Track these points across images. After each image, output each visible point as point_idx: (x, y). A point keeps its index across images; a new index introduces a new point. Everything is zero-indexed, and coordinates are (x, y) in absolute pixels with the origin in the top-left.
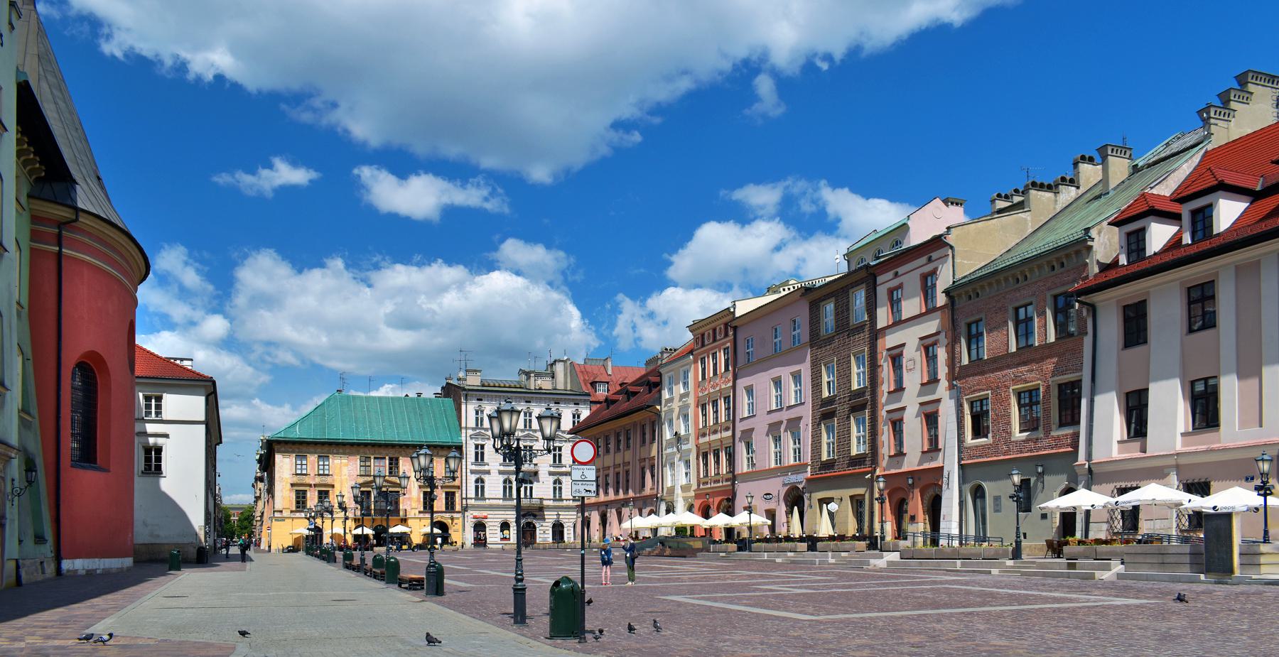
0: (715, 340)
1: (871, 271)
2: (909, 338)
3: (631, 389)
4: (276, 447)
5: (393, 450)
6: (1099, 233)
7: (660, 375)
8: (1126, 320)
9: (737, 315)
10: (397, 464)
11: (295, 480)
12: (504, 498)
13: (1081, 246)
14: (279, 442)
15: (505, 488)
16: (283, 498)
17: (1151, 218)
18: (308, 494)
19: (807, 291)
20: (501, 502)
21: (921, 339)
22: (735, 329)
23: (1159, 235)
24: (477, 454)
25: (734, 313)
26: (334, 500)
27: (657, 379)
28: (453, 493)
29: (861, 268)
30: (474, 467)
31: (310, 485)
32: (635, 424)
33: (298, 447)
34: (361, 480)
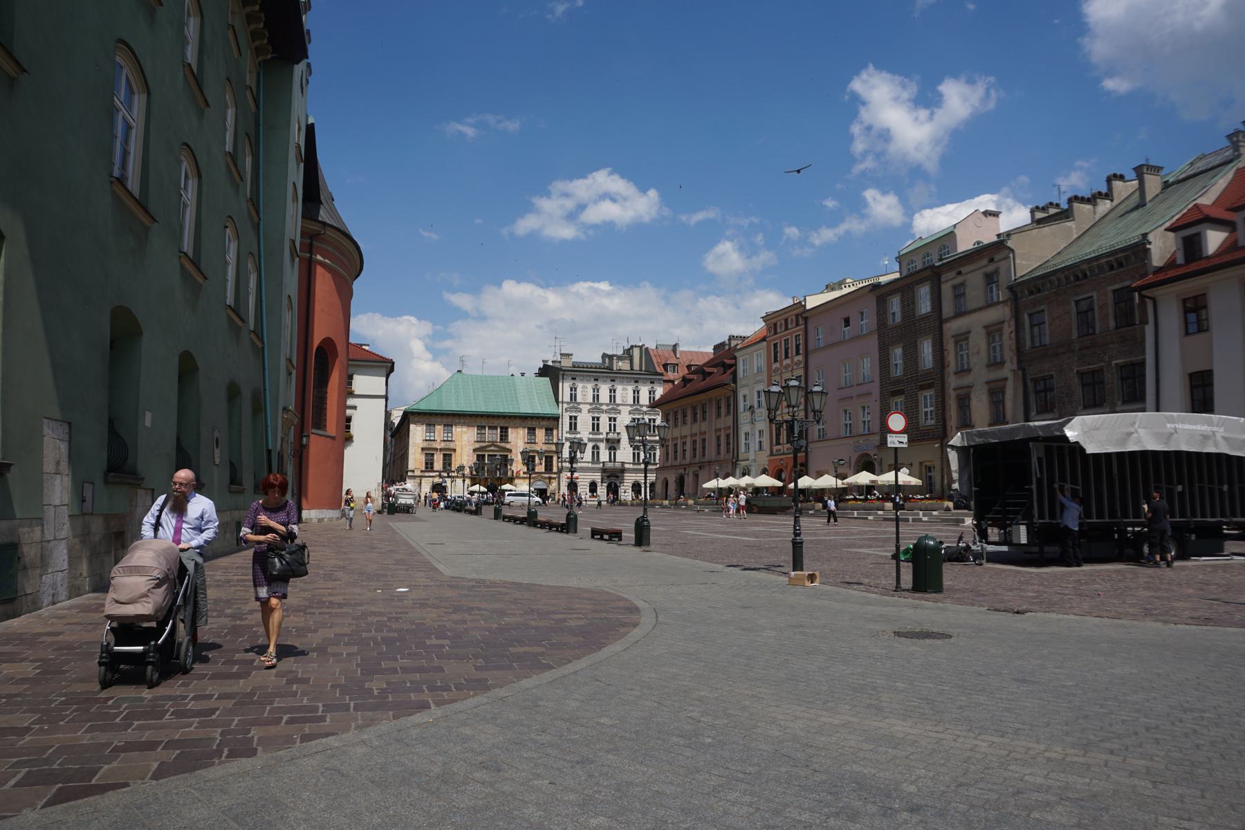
0: (786, 329)
2: (975, 323)
3: (708, 370)
4: (411, 418)
5: (502, 421)
7: (735, 358)
8: (1186, 311)
11: (425, 445)
12: (593, 462)
13: (1140, 249)
17: (1204, 225)
19: (876, 287)
21: (985, 327)
22: (806, 319)
23: (1214, 239)
32: (711, 400)
33: (429, 417)
34: (478, 445)
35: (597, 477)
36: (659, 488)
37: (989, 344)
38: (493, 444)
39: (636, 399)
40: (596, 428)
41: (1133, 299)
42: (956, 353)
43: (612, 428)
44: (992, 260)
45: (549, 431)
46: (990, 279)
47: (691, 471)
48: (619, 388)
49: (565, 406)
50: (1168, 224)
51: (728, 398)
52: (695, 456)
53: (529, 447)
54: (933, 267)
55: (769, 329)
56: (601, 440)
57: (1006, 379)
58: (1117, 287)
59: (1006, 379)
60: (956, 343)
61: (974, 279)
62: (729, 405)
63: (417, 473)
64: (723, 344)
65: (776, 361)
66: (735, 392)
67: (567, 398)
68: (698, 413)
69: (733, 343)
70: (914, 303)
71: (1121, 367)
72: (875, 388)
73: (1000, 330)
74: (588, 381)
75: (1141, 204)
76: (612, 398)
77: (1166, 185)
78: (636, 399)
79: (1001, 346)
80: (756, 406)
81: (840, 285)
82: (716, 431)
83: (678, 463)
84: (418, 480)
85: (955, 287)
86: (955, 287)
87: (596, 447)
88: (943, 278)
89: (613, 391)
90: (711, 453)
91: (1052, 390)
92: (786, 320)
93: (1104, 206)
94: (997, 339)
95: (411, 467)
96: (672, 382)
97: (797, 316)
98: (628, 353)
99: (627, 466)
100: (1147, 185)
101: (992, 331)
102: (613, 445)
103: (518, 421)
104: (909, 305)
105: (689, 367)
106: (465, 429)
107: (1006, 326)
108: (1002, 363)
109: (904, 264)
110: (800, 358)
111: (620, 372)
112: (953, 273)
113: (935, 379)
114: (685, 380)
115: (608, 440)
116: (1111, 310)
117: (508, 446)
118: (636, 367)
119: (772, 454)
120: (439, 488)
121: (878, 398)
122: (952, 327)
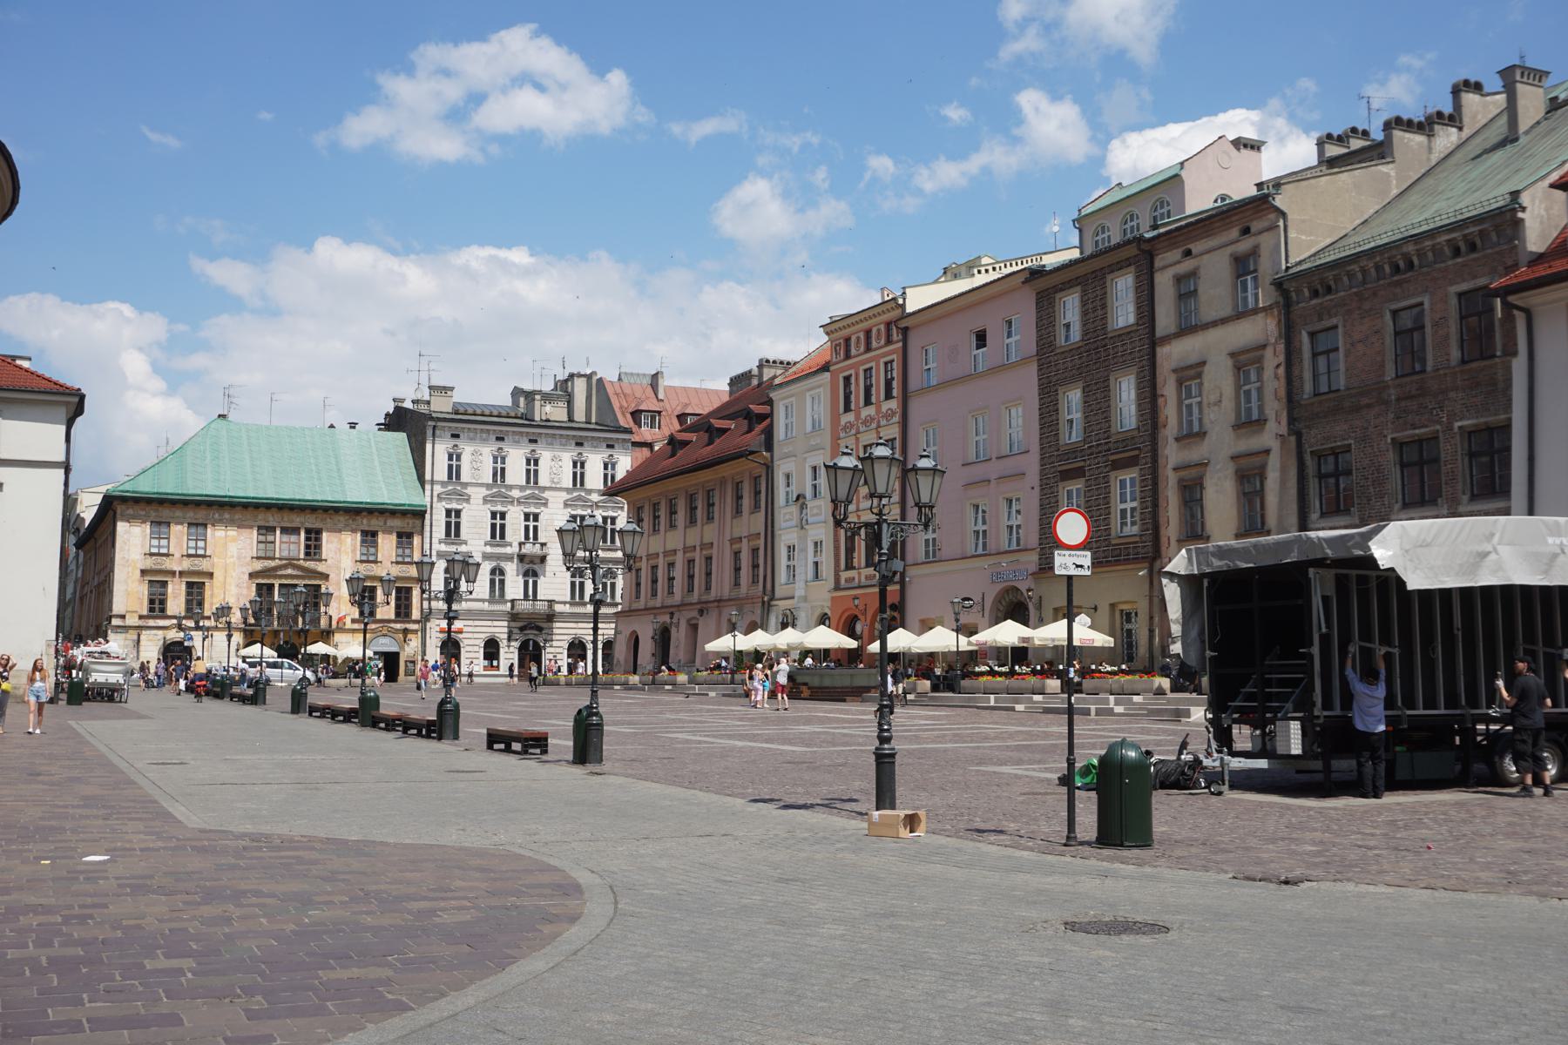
0: (868, 349)
1: (1145, 247)
2: (1214, 347)
5: (312, 518)
6: (1533, 200)
7: (770, 402)
9: (909, 309)
10: (318, 539)
11: (149, 563)
12: (491, 600)
13: (1506, 220)
14: (124, 500)
15: (492, 582)
16: (128, 594)
18: (170, 587)
19: (1036, 274)
20: (486, 606)
21: (1232, 355)
22: (905, 331)
24: (448, 524)
25: (903, 306)
26: (213, 599)
27: (764, 409)
28: (409, 590)
29: (1129, 242)
30: (443, 547)
31: (173, 573)
32: (723, 482)
33: (159, 508)
34: (258, 566)
35: (500, 629)
36: (621, 652)
37: (1238, 387)
38: (290, 562)
39: (579, 479)
40: (498, 532)
41: (1492, 310)
42: (1180, 402)
43: (531, 534)
44: (1246, 231)
45: (404, 537)
46: (1243, 266)
47: (683, 618)
48: (545, 456)
49: (438, 489)
50: (1554, 177)
51: (756, 479)
52: (691, 589)
53: (364, 570)
54: (1140, 240)
55: (835, 348)
56: (509, 558)
57: (1267, 452)
58: (1464, 287)
59: (1267, 452)
60: (1180, 383)
61: (1214, 266)
62: (757, 493)
63: (132, 620)
64: (747, 376)
65: (847, 409)
66: (769, 468)
67: (441, 474)
68: (700, 507)
69: (768, 374)
70: (1104, 306)
71: (1469, 434)
72: (1032, 465)
73: (1260, 360)
74: (485, 440)
75: (1511, 139)
76: (532, 476)
77: (1554, 105)
78: (579, 479)
79: (1260, 390)
80: (809, 493)
81: (971, 267)
82: (733, 541)
83: (658, 602)
84: (133, 635)
85: (1179, 279)
86: (1179, 279)
87: (498, 572)
88: (1158, 263)
89: (532, 461)
90: (722, 585)
91: (1349, 473)
92: (868, 333)
93: (1447, 138)
94: (1253, 377)
95: (118, 607)
96: (650, 445)
97: (888, 324)
98: (564, 389)
99: (558, 608)
100: (1522, 103)
101: (1245, 361)
102: (532, 567)
103: (342, 518)
104: (1096, 309)
105: (681, 417)
106: (232, 532)
107: (1269, 352)
108: (1261, 422)
109: (1088, 235)
110: (893, 404)
111: (547, 424)
112: (1175, 254)
113: (1140, 453)
114: (674, 443)
115: (522, 558)
116: (1453, 328)
117: (321, 567)
118: (580, 415)
119: (837, 587)
120: (176, 653)
121: (1036, 482)
122: (1173, 354)
